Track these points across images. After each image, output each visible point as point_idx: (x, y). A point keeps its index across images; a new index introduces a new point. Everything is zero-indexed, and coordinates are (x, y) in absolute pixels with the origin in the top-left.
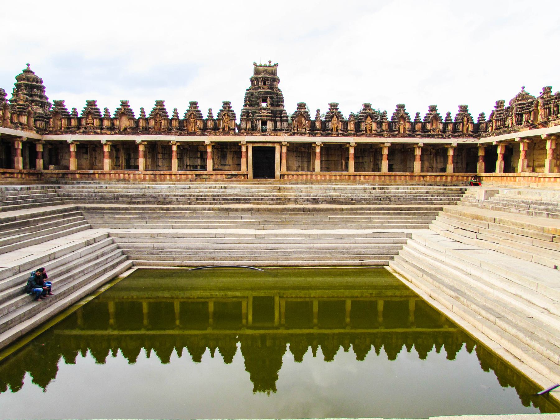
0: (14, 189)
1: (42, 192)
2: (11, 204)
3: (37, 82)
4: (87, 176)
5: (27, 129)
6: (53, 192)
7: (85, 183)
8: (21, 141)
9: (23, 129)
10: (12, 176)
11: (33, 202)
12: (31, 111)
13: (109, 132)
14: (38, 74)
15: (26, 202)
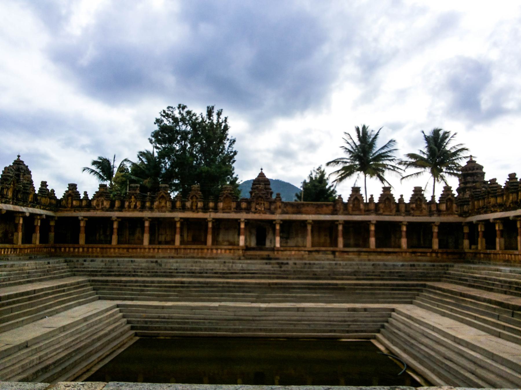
0: (394, 265)
1: (427, 269)
2: (371, 275)
3: (474, 169)
4: (486, 255)
5: (444, 214)
6: (442, 269)
7: (482, 263)
8: (436, 225)
9: (439, 215)
10: (423, 254)
11: (400, 276)
12: (452, 198)
13: (499, 210)
14: (479, 162)
15: (390, 276)
